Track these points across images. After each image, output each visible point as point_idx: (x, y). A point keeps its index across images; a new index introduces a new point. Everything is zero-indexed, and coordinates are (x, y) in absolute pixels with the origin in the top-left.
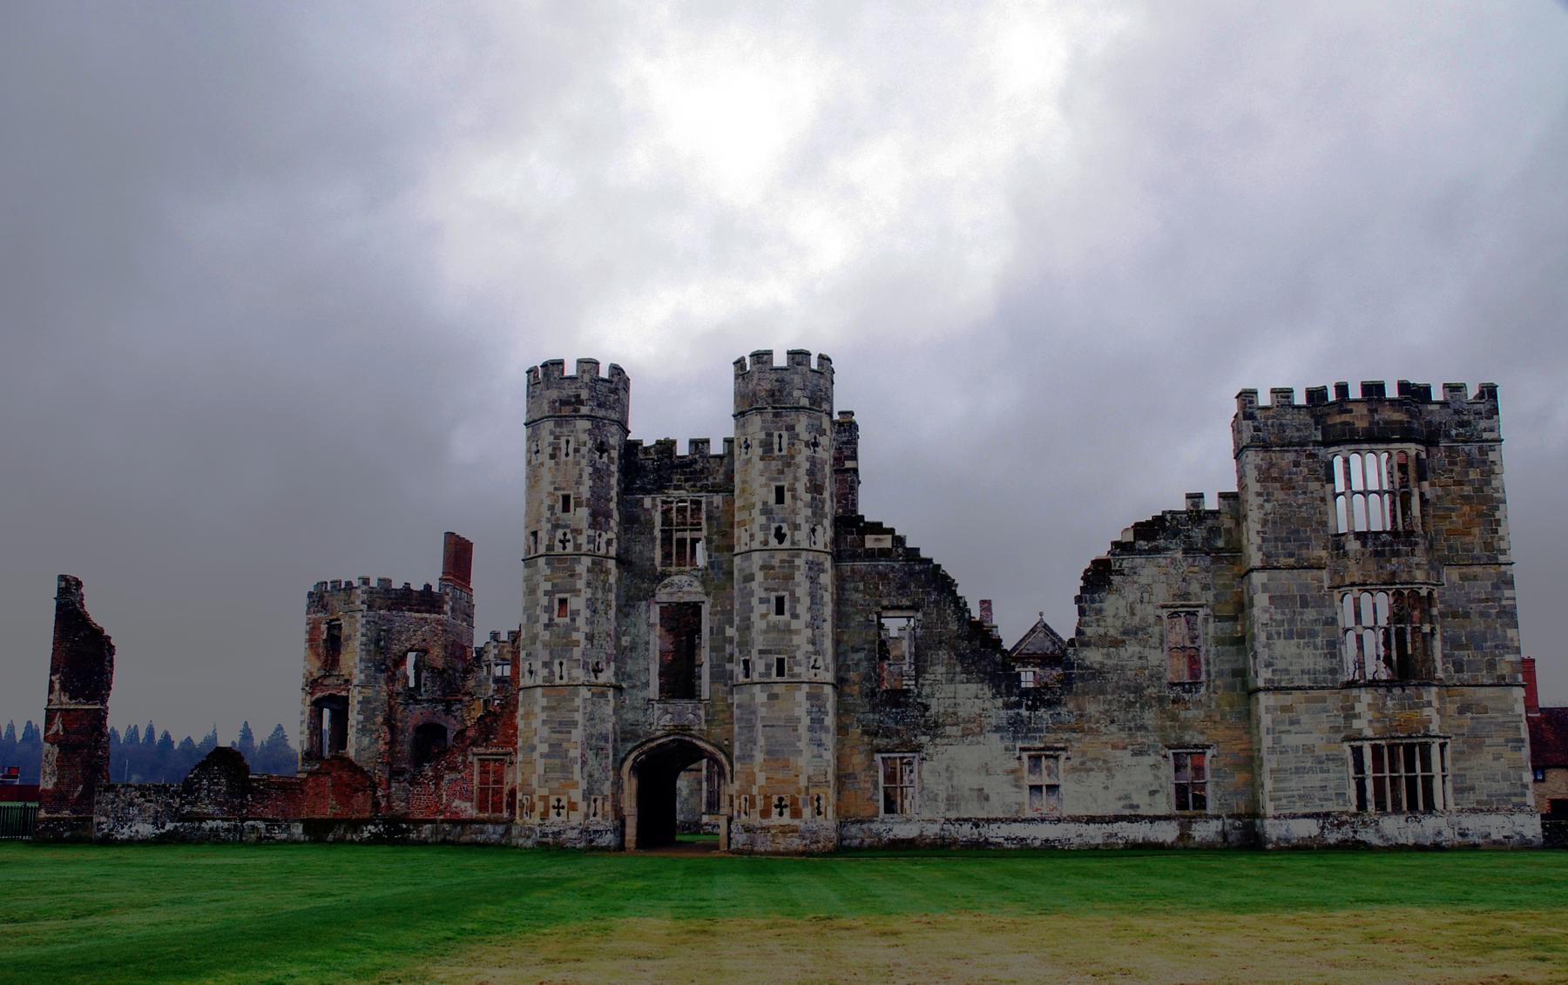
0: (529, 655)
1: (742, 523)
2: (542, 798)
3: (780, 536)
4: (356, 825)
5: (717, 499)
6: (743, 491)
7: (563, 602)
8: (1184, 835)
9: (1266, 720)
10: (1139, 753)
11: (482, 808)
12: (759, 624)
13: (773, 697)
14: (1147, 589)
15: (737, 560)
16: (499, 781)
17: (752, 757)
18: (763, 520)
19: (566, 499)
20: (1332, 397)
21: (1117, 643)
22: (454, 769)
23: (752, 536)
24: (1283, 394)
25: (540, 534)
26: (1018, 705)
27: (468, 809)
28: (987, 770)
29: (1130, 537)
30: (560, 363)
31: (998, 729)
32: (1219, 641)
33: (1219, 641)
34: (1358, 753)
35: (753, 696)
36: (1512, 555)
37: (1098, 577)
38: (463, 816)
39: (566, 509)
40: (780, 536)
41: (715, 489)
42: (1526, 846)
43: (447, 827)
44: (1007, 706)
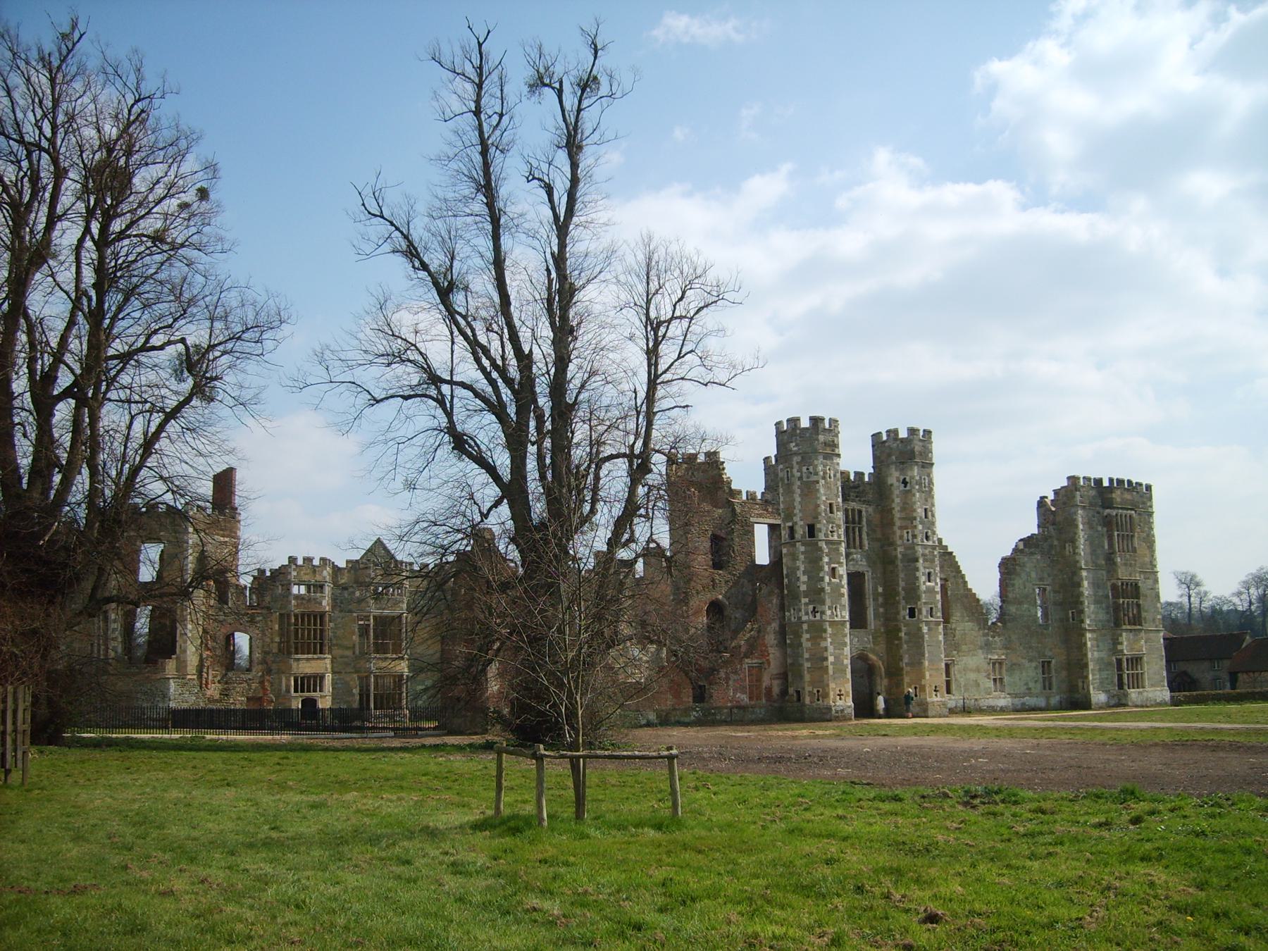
0: (811, 602)
1: (901, 528)
2: (834, 689)
3: (927, 538)
4: (687, 711)
5: (870, 509)
6: (903, 509)
7: (834, 569)
8: (1048, 703)
9: (1089, 644)
10: (1030, 661)
11: (751, 698)
12: (923, 588)
13: (930, 630)
14: (1029, 575)
15: (899, 549)
16: (759, 680)
17: (920, 664)
18: (920, 527)
19: (831, 505)
20: (1106, 483)
21: (1020, 603)
22: (736, 673)
23: (914, 536)
24: (1089, 479)
25: (818, 526)
26: (987, 635)
27: (744, 698)
28: (978, 670)
29: (1021, 546)
30: (822, 419)
31: (981, 648)
32: (1055, 604)
33: (1055, 604)
34: (1119, 662)
35: (920, 629)
36: (1159, 568)
37: (1008, 567)
38: (743, 704)
39: (831, 512)
40: (927, 538)
41: (868, 503)
42: (1166, 704)
43: (735, 711)
44: (985, 635)
